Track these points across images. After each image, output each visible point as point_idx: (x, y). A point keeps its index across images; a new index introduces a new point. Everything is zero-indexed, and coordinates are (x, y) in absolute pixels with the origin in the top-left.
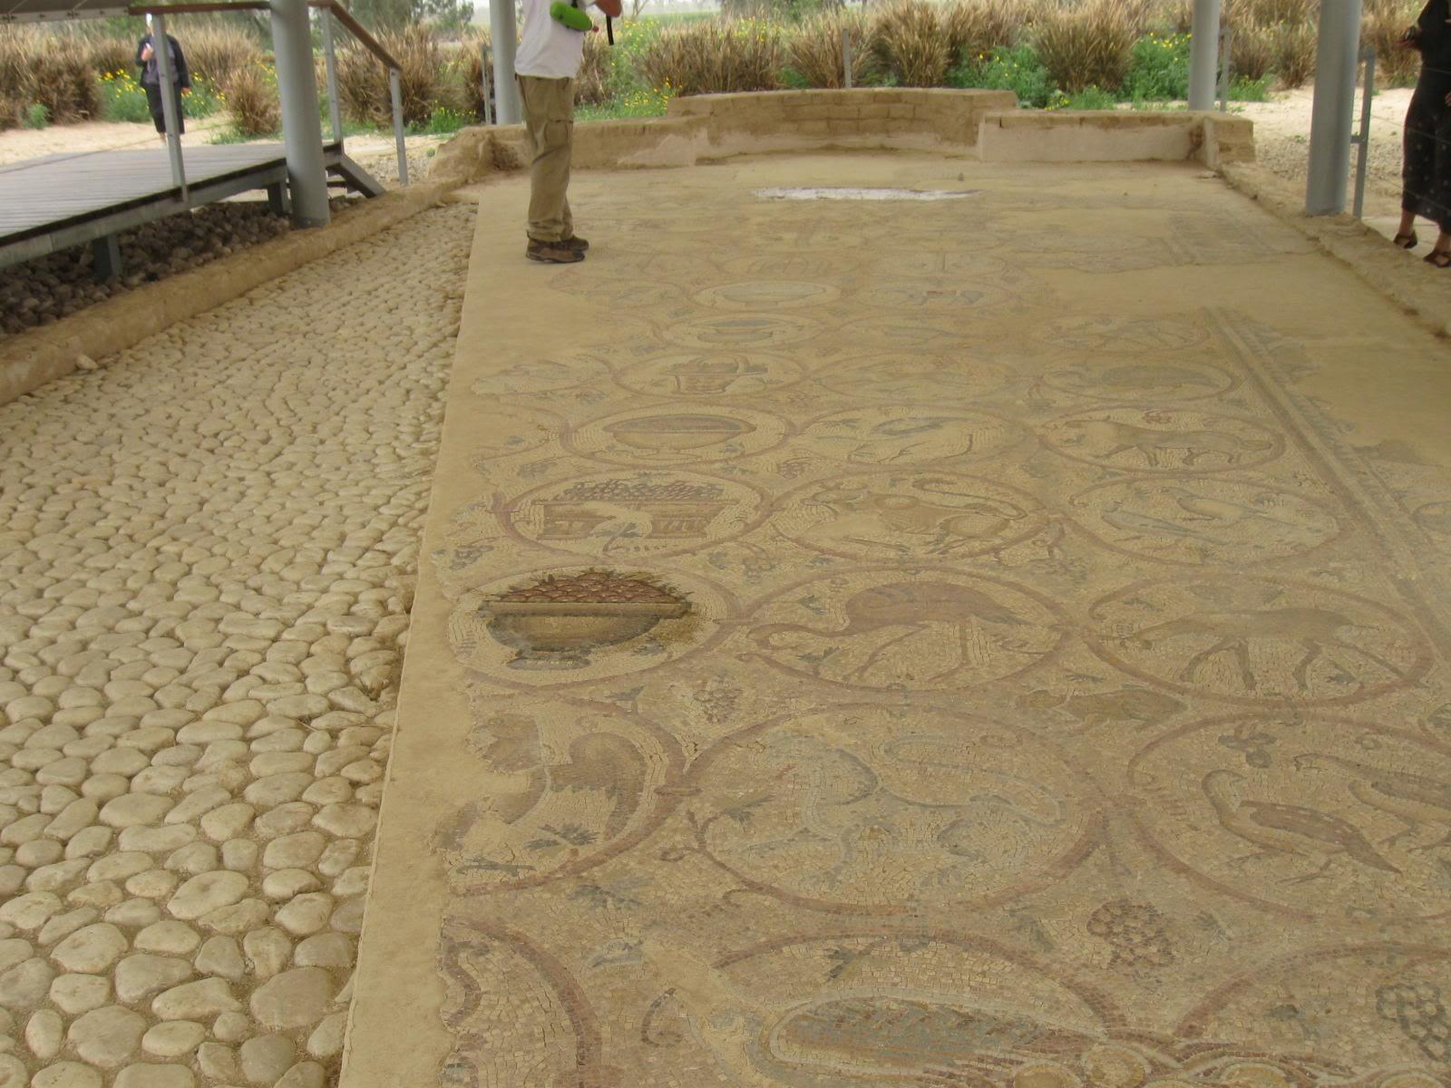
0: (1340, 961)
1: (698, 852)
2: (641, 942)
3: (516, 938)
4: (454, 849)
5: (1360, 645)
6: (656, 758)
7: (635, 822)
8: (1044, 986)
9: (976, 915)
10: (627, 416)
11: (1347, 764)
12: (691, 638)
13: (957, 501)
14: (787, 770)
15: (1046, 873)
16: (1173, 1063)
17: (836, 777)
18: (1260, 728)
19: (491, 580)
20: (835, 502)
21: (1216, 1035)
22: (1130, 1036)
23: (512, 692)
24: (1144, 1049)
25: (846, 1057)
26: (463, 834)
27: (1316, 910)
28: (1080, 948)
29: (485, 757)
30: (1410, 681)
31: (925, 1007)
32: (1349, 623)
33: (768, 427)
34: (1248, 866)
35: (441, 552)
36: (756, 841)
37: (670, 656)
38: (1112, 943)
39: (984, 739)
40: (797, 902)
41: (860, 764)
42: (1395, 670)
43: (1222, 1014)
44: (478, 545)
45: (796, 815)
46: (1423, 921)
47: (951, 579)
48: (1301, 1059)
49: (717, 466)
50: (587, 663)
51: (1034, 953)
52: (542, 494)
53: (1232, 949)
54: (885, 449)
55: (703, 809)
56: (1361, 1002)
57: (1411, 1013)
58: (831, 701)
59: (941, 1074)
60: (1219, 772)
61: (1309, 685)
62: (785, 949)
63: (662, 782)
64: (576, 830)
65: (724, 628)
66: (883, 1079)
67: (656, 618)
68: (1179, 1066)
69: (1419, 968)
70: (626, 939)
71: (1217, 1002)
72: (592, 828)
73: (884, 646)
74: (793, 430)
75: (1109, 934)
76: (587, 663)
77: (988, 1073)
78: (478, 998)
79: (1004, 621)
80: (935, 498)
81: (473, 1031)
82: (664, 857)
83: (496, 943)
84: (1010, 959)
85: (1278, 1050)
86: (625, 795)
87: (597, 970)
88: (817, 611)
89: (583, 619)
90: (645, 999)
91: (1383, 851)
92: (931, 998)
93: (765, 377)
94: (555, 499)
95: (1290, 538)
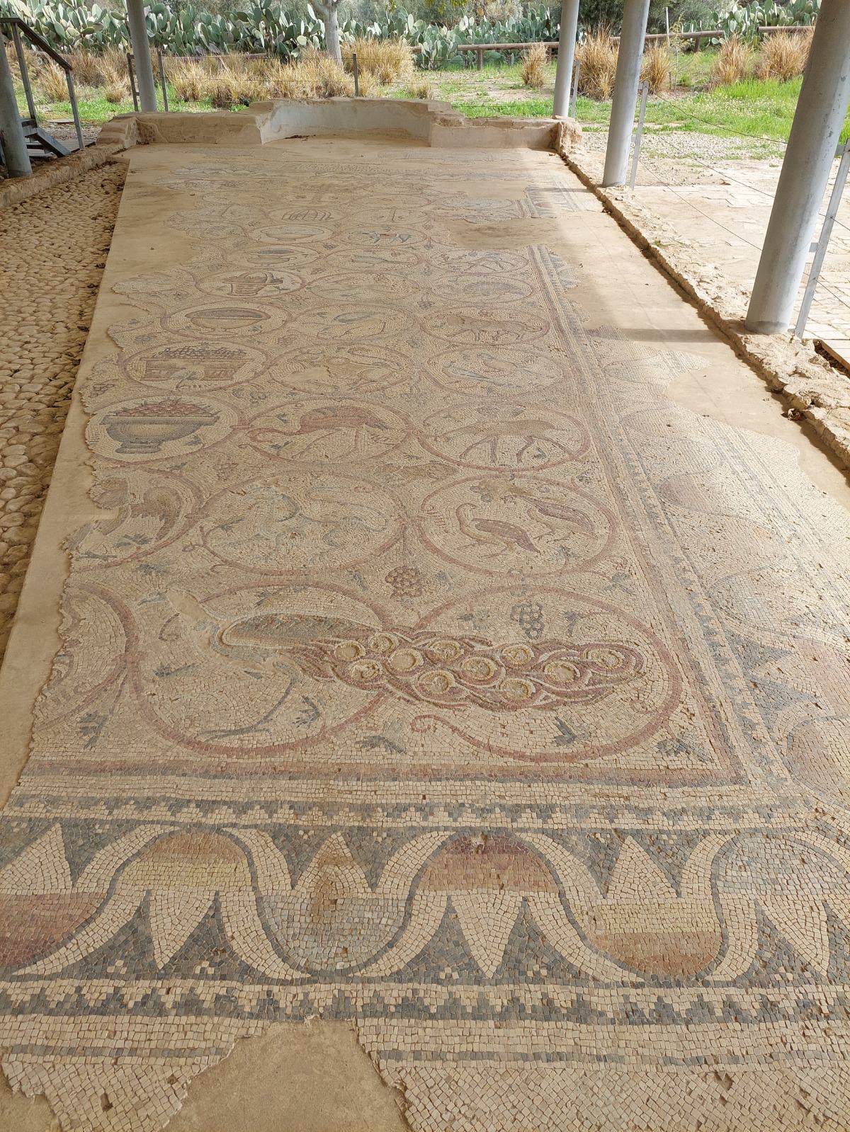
10: (200, 308)
13: (371, 361)
28: (380, 588)
33: (277, 316)
52: (146, 355)
55: (208, 524)
57: (526, 617)
74: (291, 319)
80: (358, 359)
86: (169, 518)
88: (285, 421)
93: (281, 286)
95: (537, 381)
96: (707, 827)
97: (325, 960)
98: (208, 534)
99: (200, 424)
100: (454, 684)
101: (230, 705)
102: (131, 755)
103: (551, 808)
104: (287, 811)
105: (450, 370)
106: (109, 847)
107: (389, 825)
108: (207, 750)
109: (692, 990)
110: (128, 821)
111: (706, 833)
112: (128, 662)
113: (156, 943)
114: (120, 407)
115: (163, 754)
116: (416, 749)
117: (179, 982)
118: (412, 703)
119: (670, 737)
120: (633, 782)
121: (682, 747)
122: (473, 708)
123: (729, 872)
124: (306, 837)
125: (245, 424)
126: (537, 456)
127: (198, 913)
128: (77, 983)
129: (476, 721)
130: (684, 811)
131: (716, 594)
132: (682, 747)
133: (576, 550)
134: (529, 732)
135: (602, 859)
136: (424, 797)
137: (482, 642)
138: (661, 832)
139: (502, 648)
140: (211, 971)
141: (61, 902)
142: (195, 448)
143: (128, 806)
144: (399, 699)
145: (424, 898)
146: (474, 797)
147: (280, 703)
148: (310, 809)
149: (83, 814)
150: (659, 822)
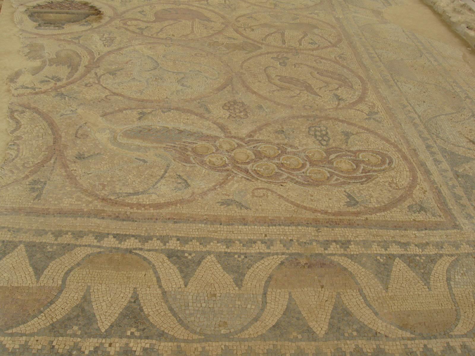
0: (299, 119)
1: (98, 84)
2: (76, 109)
3: (34, 108)
4: (14, 83)
5: (320, 34)
6: (85, 57)
8: (206, 123)
9: (187, 103)
11: (310, 67)
12: (99, 21)
15: (211, 92)
16: (244, 144)
17: (145, 63)
18: (285, 55)
21: (258, 137)
22: (232, 137)
23: (36, 36)
24: (235, 140)
25: (141, 141)
26: (17, 78)
27: (294, 106)
28: (218, 112)
29: (25, 56)
30: (334, 45)
31: (168, 128)
32: (318, 28)
34: (275, 93)
36: (117, 81)
37: (92, 26)
38: (230, 112)
39: (196, 54)
40: (129, 98)
41: (154, 60)
42: (330, 42)
43: (261, 132)
45: (132, 74)
46: (326, 110)
47: (191, 8)
48: (283, 144)
50: (63, 28)
51: (204, 114)
53: (266, 115)
55: (100, 71)
56: (304, 130)
57: (318, 133)
58: (146, 41)
59: (171, 146)
60: (270, 67)
61: (303, 45)
62: (124, 112)
63: (87, 63)
64: (56, 77)
65: (112, 19)
66: (153, 147)
67: (88, 15)
68: (246, 145)
69: (322, 122)
70: (71, 109)
71: (260, 129)
72: (62, 77)
73: (166, 26)
75: (229, 109)
76: (63, 28)
77: (186, 146)
78: (21, 126)
79: (207, 21)
81: (19, 135)
82: (86, 85)
83: (27, 110)
84: (197, 115)
85: (276, 142)
86: (74, 67)
87: (61, 117)
88: (145, 15)
89: (62, 15)
90: (77, 125)
91: (317, 91)
92: (171, 126)
96: (441, 252)
97: (213, 328)
98: (100, 77)
100: (277, 170)
101: (128, 178)
102: (66, 204)
103: (349, 242)
104: (175, 242)
106: (57, 260)
107: (245, 251)
108: (116, 204)
109: (443, 340)
110: (69, 245)
111: (441, 256)
112: (55, 151)
113: (98, 317)
115: (87, 205)
116: (257, 207)
117: (117, 340)
118: (250, 181)
119: (414, 203)
120: (395, 228)
122: (291, 185)
123: (457, 277)
124: (190, 257)
126: (312, 43)
127: (123, 300)
128: (49, 339)
129: (294, 192)
130: (428, 244)
131: (429, 126)
132: (422, 209)
133: (344, 97)
134: (330, 199)
135: (383, 269)
136: (266, 236)
137: (291, 146)
138: (416, 255)
139: (304, 151)
140: (137, 334)
141: (31, 291)
143: (67, 236)
145: (274, 293)
146: (299, 236)
147: (162, 178)
148: (191, 240)
149: (37, 240)
150: (413, 250)
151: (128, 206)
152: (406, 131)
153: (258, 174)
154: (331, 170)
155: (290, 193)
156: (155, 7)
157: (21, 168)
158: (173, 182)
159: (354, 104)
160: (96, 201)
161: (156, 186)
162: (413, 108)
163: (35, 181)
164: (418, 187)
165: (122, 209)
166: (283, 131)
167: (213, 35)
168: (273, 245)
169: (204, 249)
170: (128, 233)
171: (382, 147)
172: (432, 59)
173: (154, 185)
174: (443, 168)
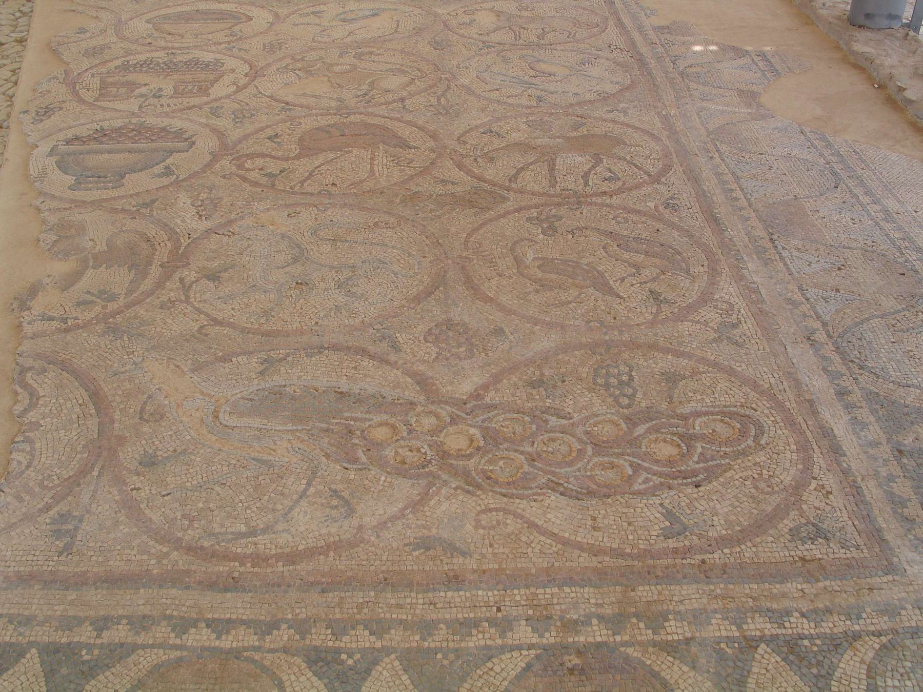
6: (162, 244)
7: (147, 285)
10: (163, 12)
14: (246, 248)
16: (464, 415)
19: (60, 130)
20: (299, 70)
24: (447, 407)
26: (32, 299)
30: (656, 179)
35: (27, 112)
39: (376, 224)
40: (244, 331)
44: (52, 106)
47: (370, 120)
49: (223, 46)
53: (511, 348)
54: (339, 33)
55: (190, 275)
58: (281, 202)
71: (497, 379)
73: (319, 166)
81: (33, 420)
90: (144, 393)
91: (615, 286)
94: (108, 72)
95: (598, 88)
98: (190, 286)
99: (171, 152)
100: (526, 468)
101: (237, 500)
105: (486, 75)
108: (212, 556)
110: (122, 645)
112: (103, 450)
114: (70, 134)
116: (484, 551)
120: (759, 578)
121: (819, 533)
122: (553, 498)
124: (350, 662)
125: (225, 148)
129: (557, 514)
132: (819, 533)
136: (499, 610)
142: (165, 181)
143: (120, 627)
144: (456, 489)
146: (563, 607)
151: (234, 560)
152: (794, 361)
153: (489, 478)
154: (636, 460)
155: (549, 516)
156: (300, 124)
157: (37, 489)
158: (322, 505)
159: (691, 308)
160: (176, 553)
161: (290, 515)
162: (813, 308)
163: (63, 515)
164: (814, 484)
165: (223, 568)
166: (543, 382)
167: (412, 177)
168: (512, 630)
169: (378, 645)
170: (234, 617)
171: (743, 400)
172: (859, 191)
173: (286, 514)
174: (870, 438)
